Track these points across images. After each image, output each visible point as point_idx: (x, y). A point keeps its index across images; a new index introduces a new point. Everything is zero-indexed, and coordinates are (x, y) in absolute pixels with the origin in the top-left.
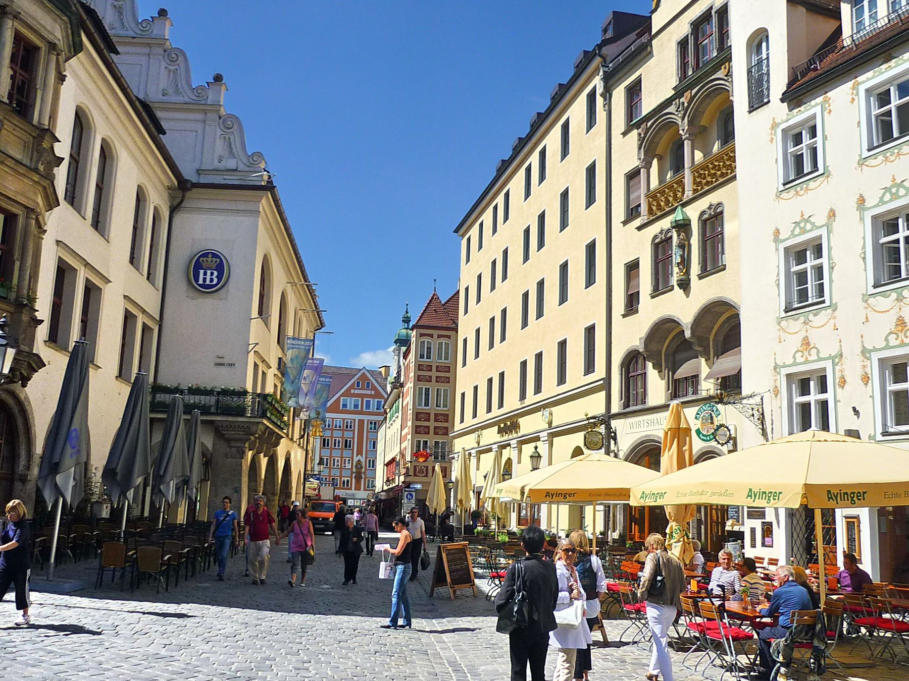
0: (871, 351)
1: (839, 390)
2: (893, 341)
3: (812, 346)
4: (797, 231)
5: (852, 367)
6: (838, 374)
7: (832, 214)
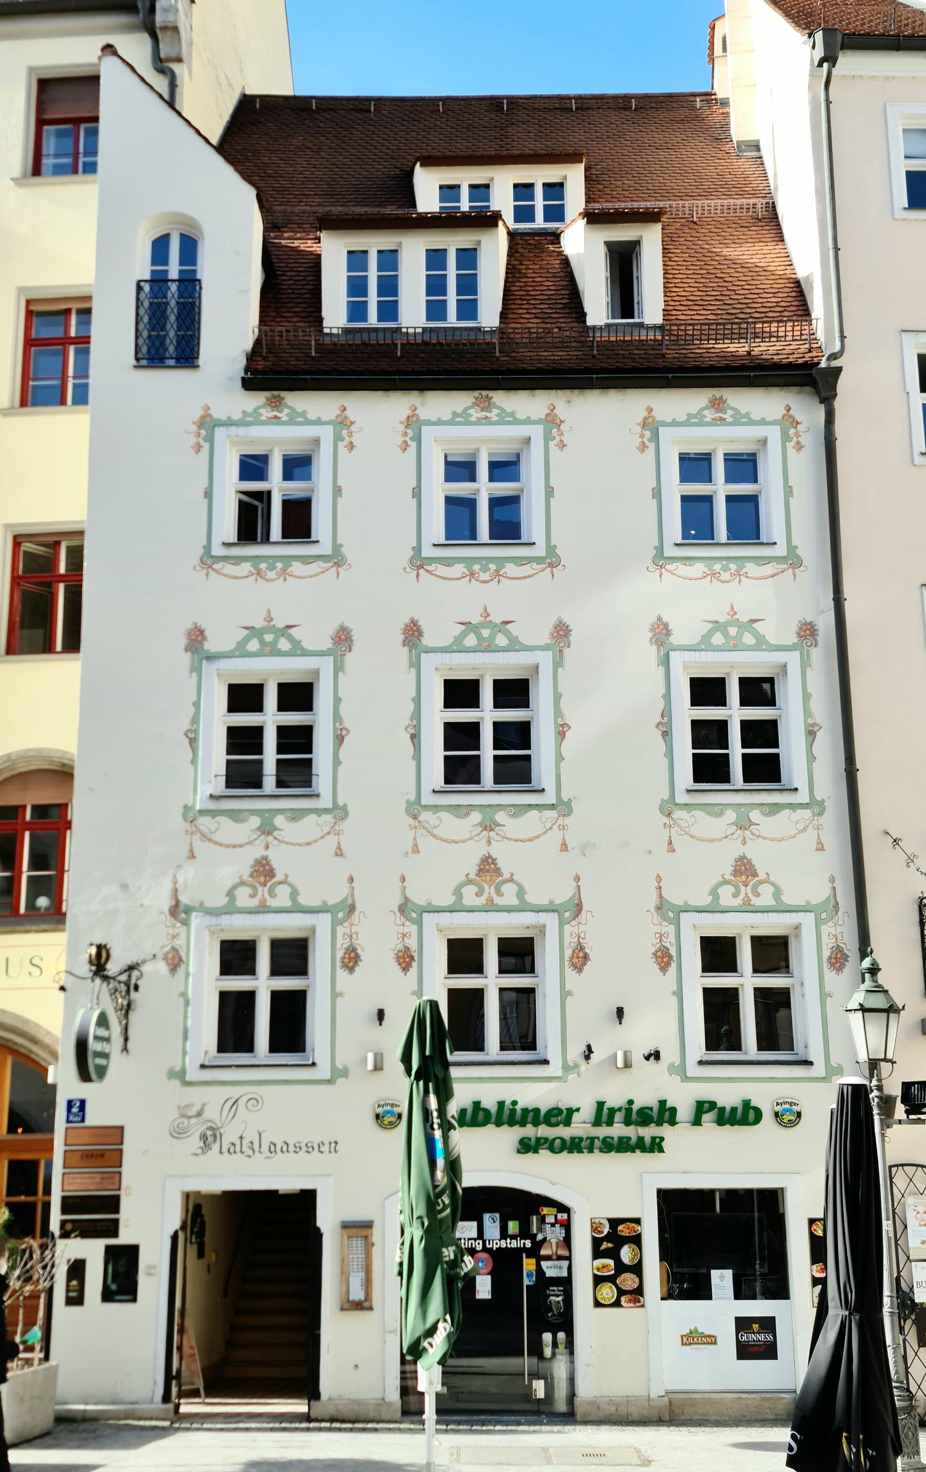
1: (342, 974)
3: (279, 877)
6: (342, 943)
7: (343, 639)
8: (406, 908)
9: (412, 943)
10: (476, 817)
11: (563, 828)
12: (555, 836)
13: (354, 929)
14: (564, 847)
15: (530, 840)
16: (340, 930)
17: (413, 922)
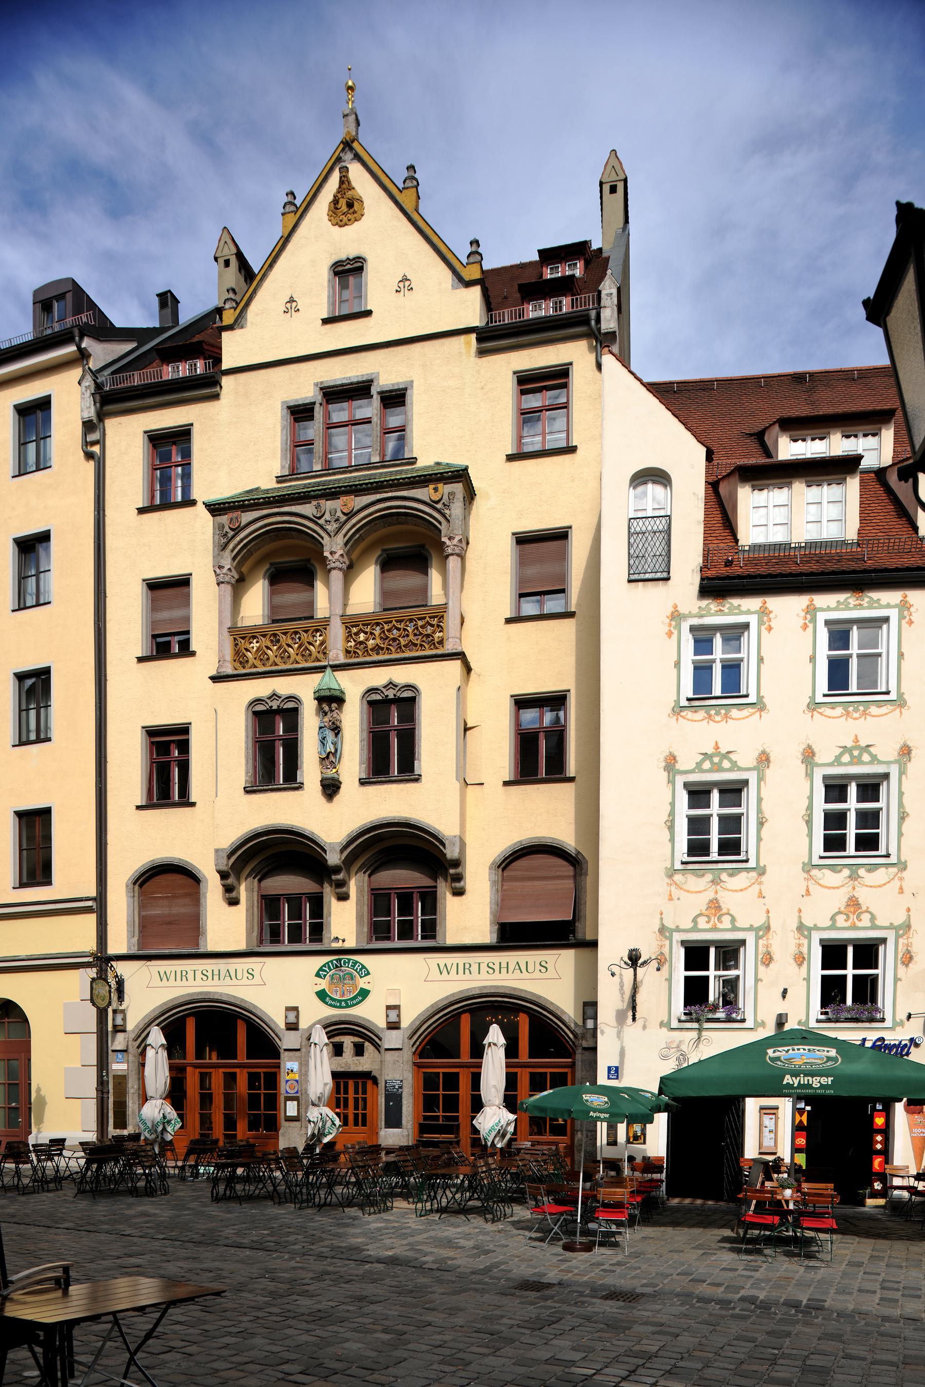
0: (810, 930)
1: (761, 968)
2: (841, 921)
4: (707, 765)
5: (784, 943)
8: (801, 928)
9: (805, 950)
10: (846, 872)
11: (901, 879)
12: (896, 883)
13: (770, 942)
14: (901, 890)
15: (880, 886)
16: (761, 942)
17: (805, 937)
